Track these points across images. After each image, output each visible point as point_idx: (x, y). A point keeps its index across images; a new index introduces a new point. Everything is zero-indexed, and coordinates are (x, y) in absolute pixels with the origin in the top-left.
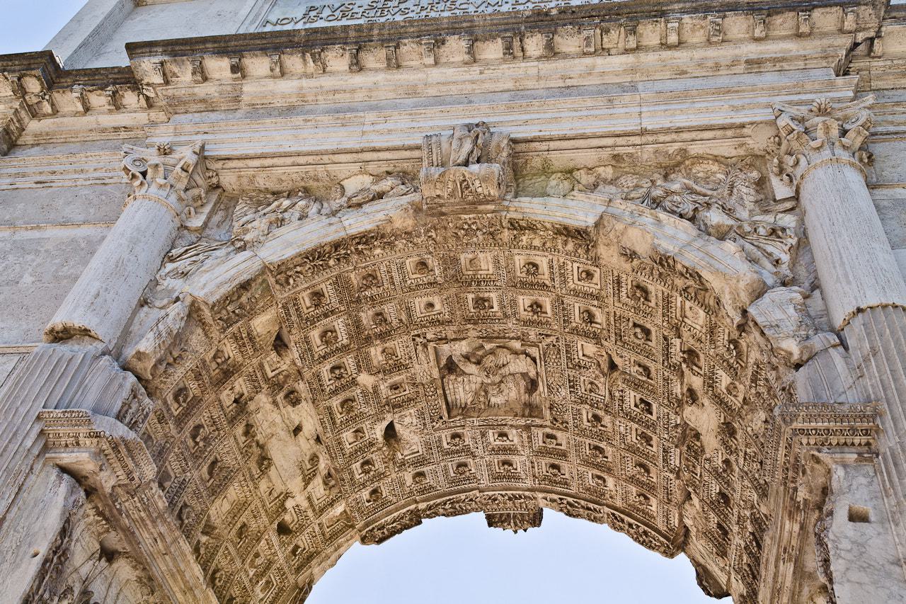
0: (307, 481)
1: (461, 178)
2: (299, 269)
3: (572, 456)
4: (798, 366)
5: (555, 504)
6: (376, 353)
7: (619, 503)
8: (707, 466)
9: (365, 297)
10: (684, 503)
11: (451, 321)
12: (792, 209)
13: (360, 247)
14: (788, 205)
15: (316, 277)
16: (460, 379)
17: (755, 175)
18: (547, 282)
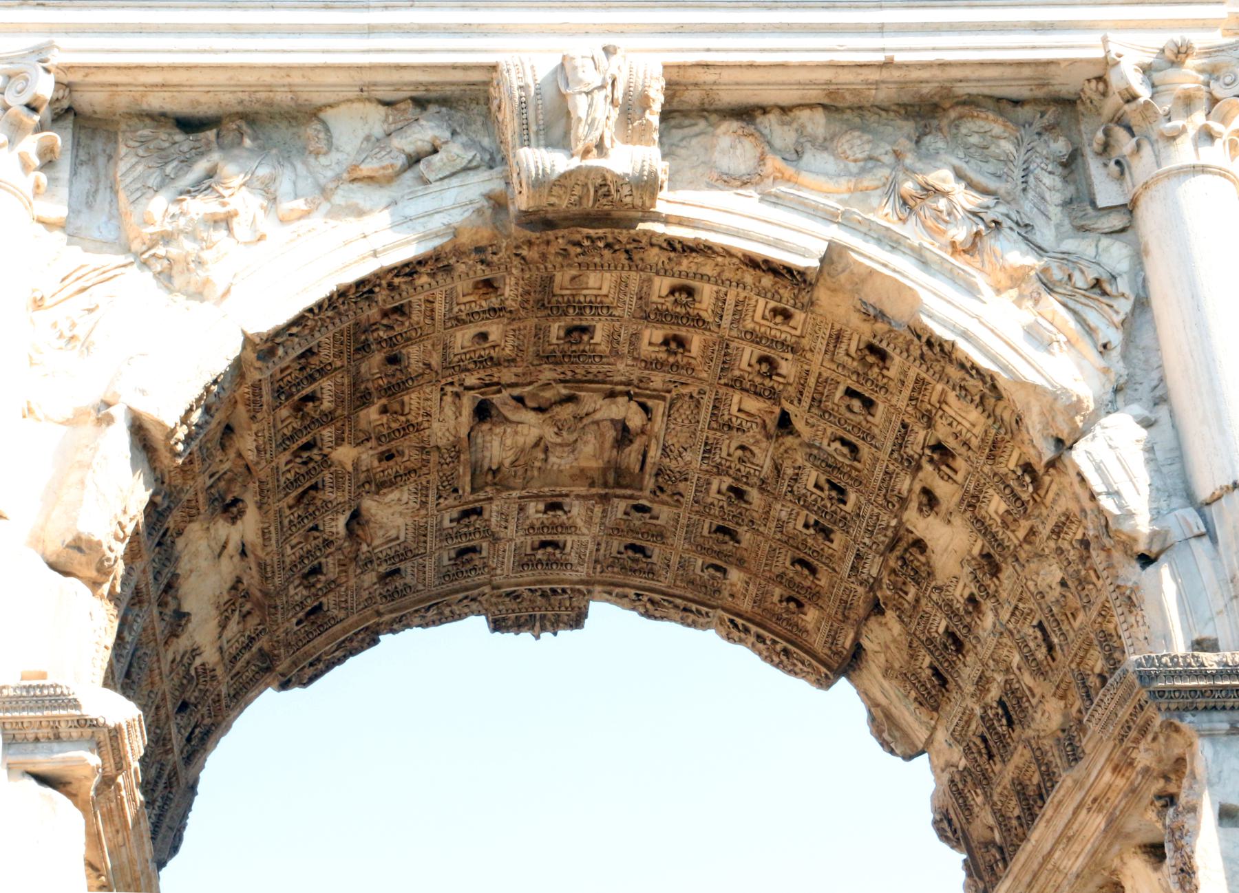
0: (223, 626)
1: (599, 181)
2: (294, 330)
3: (678, 541)
4: (1146, 560)
5: (626, 600)
6: (371, 415)
7: (746, 605)
8: (935, 597)
9: (379, 341)
10: (867, 619)
11: (514, 360)
12: (1123, 230)
13: (396, 281)
14: (1116, 221)
15: (317, 334)
16: (498, 430)
17: (1060, 146)
18: (704, 314)
